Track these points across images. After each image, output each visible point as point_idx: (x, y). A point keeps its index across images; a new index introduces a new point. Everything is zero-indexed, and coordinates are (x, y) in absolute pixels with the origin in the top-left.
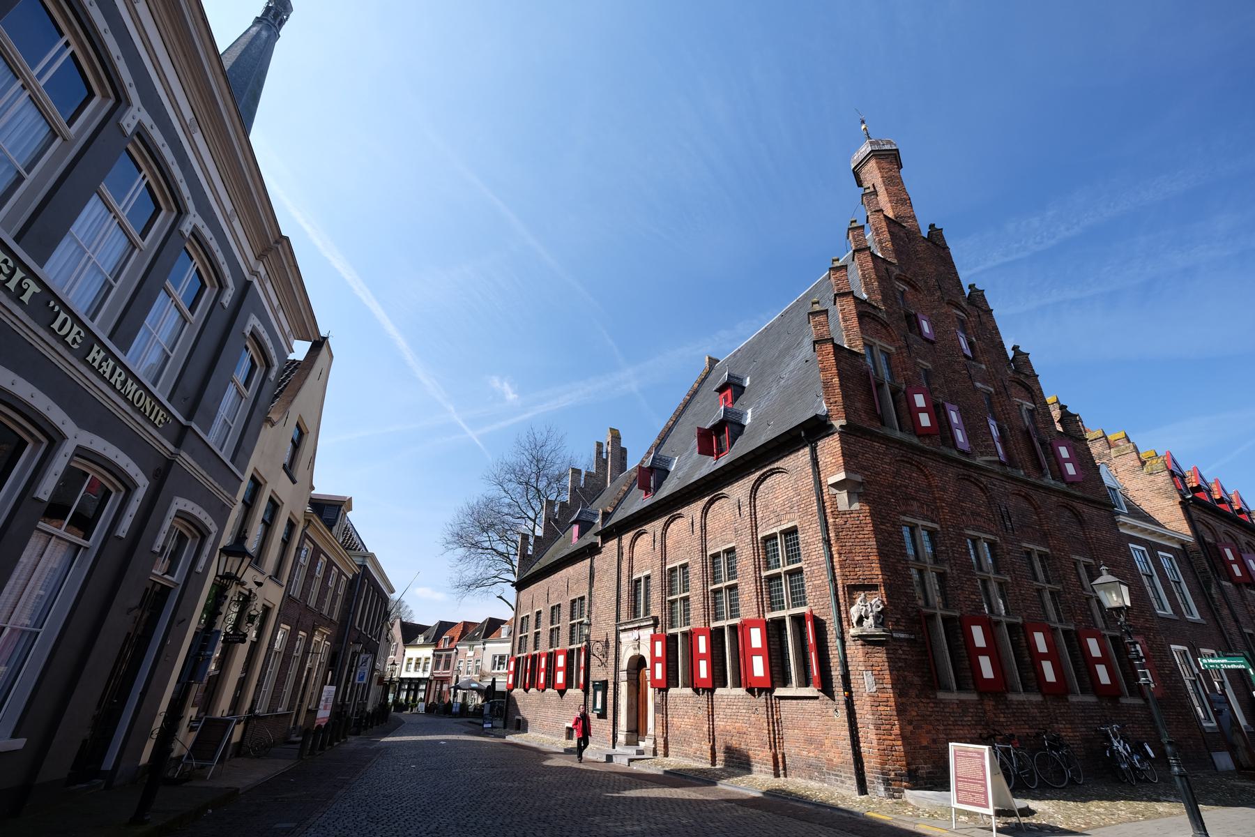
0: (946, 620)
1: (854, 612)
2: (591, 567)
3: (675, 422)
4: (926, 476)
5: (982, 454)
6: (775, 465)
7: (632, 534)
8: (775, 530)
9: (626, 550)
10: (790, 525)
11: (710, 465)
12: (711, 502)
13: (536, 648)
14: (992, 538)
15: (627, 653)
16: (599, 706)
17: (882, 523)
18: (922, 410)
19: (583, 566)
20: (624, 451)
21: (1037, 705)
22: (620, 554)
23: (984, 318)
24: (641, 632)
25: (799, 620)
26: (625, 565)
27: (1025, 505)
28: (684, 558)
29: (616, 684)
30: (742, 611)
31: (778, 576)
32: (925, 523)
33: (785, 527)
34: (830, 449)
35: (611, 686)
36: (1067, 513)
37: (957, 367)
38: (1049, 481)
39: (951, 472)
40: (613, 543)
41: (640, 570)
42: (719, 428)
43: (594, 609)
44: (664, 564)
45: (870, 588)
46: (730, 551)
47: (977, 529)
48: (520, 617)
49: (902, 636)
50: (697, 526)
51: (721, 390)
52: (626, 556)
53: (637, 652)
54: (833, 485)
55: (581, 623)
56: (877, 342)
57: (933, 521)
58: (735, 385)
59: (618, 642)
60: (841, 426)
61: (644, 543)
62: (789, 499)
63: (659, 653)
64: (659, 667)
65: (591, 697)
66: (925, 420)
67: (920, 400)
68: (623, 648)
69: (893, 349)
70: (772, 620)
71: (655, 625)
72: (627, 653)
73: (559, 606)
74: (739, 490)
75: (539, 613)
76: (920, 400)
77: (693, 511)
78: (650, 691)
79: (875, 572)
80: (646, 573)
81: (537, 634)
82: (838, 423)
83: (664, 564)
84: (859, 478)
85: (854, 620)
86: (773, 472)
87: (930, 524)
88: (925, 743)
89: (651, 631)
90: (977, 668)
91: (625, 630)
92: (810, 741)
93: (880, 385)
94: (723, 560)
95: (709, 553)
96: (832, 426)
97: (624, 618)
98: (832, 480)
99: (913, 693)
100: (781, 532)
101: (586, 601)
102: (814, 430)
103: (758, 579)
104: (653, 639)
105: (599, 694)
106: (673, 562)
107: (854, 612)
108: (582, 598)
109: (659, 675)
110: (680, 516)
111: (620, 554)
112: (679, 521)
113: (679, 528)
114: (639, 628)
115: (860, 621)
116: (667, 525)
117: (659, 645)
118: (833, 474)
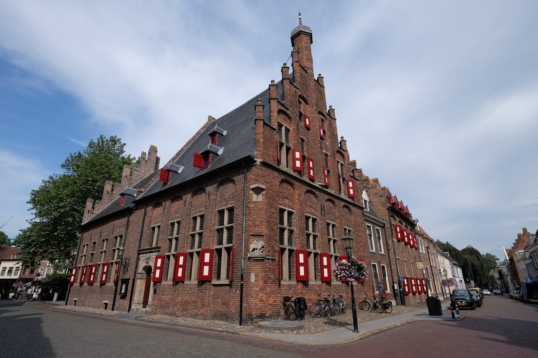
0: (289, 250)
1: (252, 246)
4: (294, 189)
5: (319, 181)
8: (224, 208)
10: (231, 206)
14: (315, 217)
15: (142, 264)
16: (123, 291)
17: (271, 208)
18: (298, 159)
21: (320, 286)
23: (333, 121)
24: (151, 254)
26: (147, 220)
27: (331, 204)
29: (134, 281)
30: (203, 245)
31: (222, 229)
32: (289, 209)
33: (228, 206)
35: (131, 281)
36: (347, 209)
37: (316, 142)
38: (343, 196)
43: (127, 242)
45: (259, 236)
46: (202, 217)
47: (311, 213)
49: (270, 257)
53: (147, 264)
54: (252, 189)
55: (118, 249)
56: (285, 125)
57: (293, 209)
58: (219, 134)
59: (138, 259)
60: (260, 162)
62: (232, 194)
63: (159, 265)
64: (158, 271)
65: (119, 287)
66: (298, 164)
67: (298, 155)
68: (141, 262)
69: (291, 129)
72: (142, 264)
75: (94, 243)
76: (298, 155)
78: (152, 283)
79: (264, 230)
80: (158, 224)
82: (258, 161)
84: (264, 187)
85: (251, 250)
87: (291, 210)
88: (271, 302)
89: (157, 254)
90: (298, 271)
91: (143, 253)
92: (224, 304)
94: (199, 220)
98: (252, 187)
99: (270, 281)
100: (227, 209)
101: (123, 238)
104: (157, 258)
105: (124, 287)
106: (173, 219)
107: (252, 246)
109: (157, 275)
114: (150, 252)
115: (254, 250)
117: (159, 261)
118: (253, 184)
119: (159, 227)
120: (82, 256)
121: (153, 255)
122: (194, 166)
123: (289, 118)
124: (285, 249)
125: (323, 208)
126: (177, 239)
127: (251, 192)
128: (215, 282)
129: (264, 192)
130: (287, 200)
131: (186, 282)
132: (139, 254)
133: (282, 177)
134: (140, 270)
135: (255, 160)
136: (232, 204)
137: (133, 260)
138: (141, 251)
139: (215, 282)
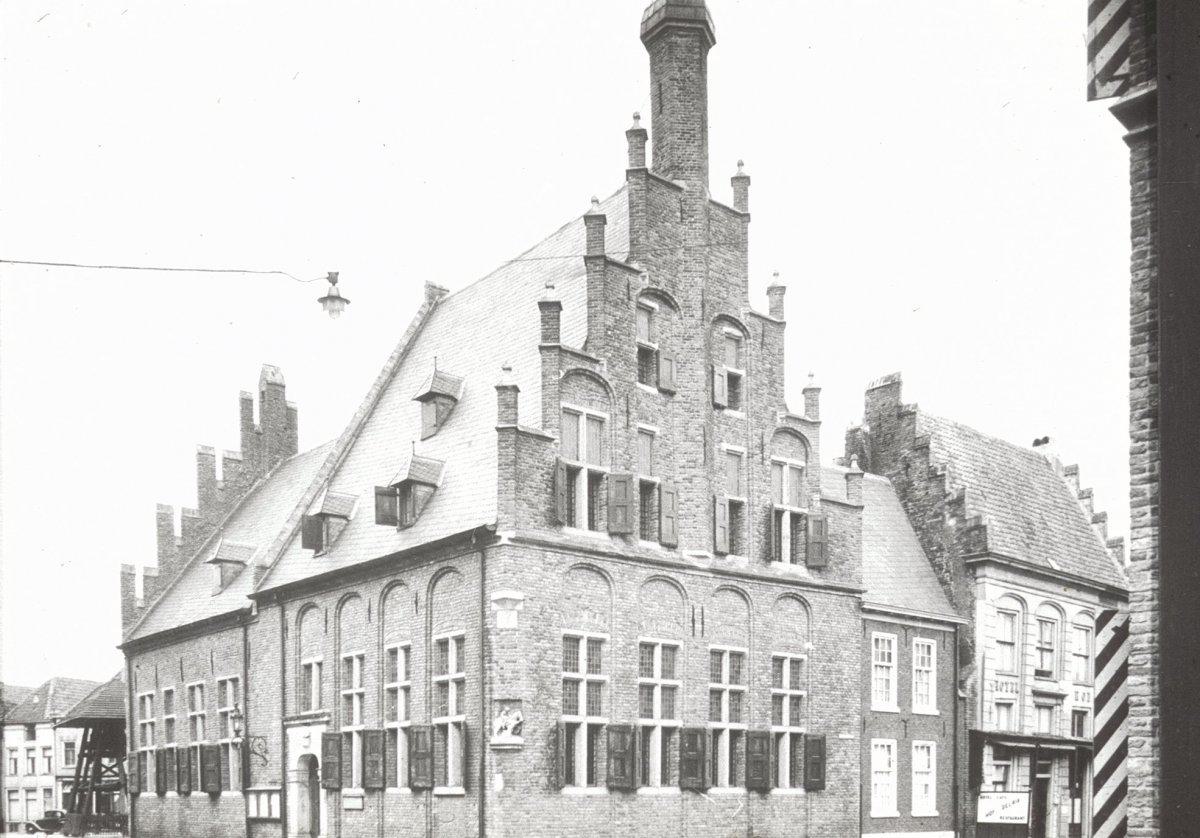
2: (245, 640)
3: (370, 414)
6: (453, 563)
7: (298, 604)
9: (291, 626)
11: (388, 541)
12: (391, 586)
13: (170, 739)
17: (538, 640)
19: (232, 639)
20: (290, 415)
22: (284, 629)
25: (457, 725)
26: (290, 644)
28: (360, 648)
34: (500, 561)
39: (644, 572)
40: (272, 616)
41: (311, 654)
42: (406, 487)
43: (252, 696)
44: (337, 652)
48: (138, 696)
50: (375, 611)
51: (427, 398)
52: (291, 634)
54: (496, 601)
60: (510, 539)
61: (313, 620)
69: (606, 416)
70: (439, 725)
71: (327, 723)
73: (201, 687)
74: (417, 581)
75: (169, 693)
77: (370, 593)
78: (323, 792)
80: (319, 658)
81: (170, 722)
82: (505, 535)
83: (337, 652)
84: (519, 595)
86: (451, 569)
93: (573, 473)
94: (401, 654)
95: (387, 647)
96: (500, 537)
97: (291, 713)
102: (480, 540)
103: (428, 683)
106: (348, 650)
107: (497, 723)
108: (235, 681)
110: (356, 595)
111: (284, 629)
112: (358, 601)
113: (354, 611)
116: (342, 602)
119: (320, 664)
120: (144, 726)
121: (317, 732)
122: (378, 522)
123: (604, 385)
124: (577, 725)
125: (698, 618)
126: (361, 696)
127: (495, 607)
128: (438, 790)
129: (520, 607)
130: (585, 615)
131: (389, 790)
132: (284, 728)
133: (571, 559)
134: (293, 763)
135: (498, 534)
136: (460, 628)
137: (275, 738)
138: (286, 720)
139: (438, 790)
